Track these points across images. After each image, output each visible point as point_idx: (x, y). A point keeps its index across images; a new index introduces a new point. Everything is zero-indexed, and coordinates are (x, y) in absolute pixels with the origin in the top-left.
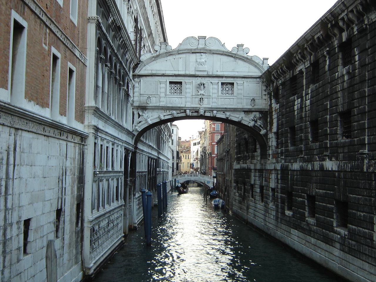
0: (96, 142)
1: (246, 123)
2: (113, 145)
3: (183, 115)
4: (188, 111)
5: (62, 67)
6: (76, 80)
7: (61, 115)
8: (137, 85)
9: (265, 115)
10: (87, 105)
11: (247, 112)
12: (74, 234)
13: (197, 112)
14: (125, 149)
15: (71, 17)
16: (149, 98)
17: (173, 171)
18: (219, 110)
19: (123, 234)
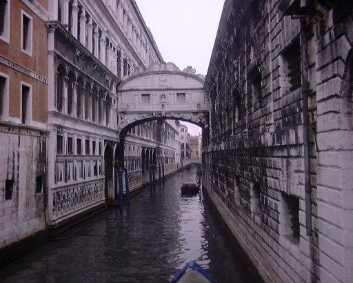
0: (62, 135)
1: (194, 121)
2: (86, 137)
3: (152, 117)
4: (154, 114)
5: (10, 84)
6: (33, 94)
7: (12, 116)
8: (120, 97)
9: (206, 113)
10: (49, 110)
11: (195, 113)
12: (33, 198)
13: (161, 114)
14: (105, 141)
15: (23, 50)
16: (127, 105)
17: (182, 156)
18: (175, 112)
19: (104, 199)
